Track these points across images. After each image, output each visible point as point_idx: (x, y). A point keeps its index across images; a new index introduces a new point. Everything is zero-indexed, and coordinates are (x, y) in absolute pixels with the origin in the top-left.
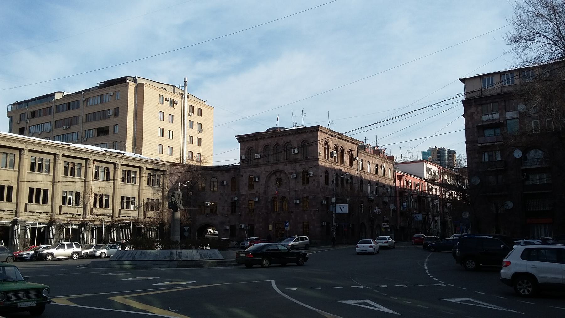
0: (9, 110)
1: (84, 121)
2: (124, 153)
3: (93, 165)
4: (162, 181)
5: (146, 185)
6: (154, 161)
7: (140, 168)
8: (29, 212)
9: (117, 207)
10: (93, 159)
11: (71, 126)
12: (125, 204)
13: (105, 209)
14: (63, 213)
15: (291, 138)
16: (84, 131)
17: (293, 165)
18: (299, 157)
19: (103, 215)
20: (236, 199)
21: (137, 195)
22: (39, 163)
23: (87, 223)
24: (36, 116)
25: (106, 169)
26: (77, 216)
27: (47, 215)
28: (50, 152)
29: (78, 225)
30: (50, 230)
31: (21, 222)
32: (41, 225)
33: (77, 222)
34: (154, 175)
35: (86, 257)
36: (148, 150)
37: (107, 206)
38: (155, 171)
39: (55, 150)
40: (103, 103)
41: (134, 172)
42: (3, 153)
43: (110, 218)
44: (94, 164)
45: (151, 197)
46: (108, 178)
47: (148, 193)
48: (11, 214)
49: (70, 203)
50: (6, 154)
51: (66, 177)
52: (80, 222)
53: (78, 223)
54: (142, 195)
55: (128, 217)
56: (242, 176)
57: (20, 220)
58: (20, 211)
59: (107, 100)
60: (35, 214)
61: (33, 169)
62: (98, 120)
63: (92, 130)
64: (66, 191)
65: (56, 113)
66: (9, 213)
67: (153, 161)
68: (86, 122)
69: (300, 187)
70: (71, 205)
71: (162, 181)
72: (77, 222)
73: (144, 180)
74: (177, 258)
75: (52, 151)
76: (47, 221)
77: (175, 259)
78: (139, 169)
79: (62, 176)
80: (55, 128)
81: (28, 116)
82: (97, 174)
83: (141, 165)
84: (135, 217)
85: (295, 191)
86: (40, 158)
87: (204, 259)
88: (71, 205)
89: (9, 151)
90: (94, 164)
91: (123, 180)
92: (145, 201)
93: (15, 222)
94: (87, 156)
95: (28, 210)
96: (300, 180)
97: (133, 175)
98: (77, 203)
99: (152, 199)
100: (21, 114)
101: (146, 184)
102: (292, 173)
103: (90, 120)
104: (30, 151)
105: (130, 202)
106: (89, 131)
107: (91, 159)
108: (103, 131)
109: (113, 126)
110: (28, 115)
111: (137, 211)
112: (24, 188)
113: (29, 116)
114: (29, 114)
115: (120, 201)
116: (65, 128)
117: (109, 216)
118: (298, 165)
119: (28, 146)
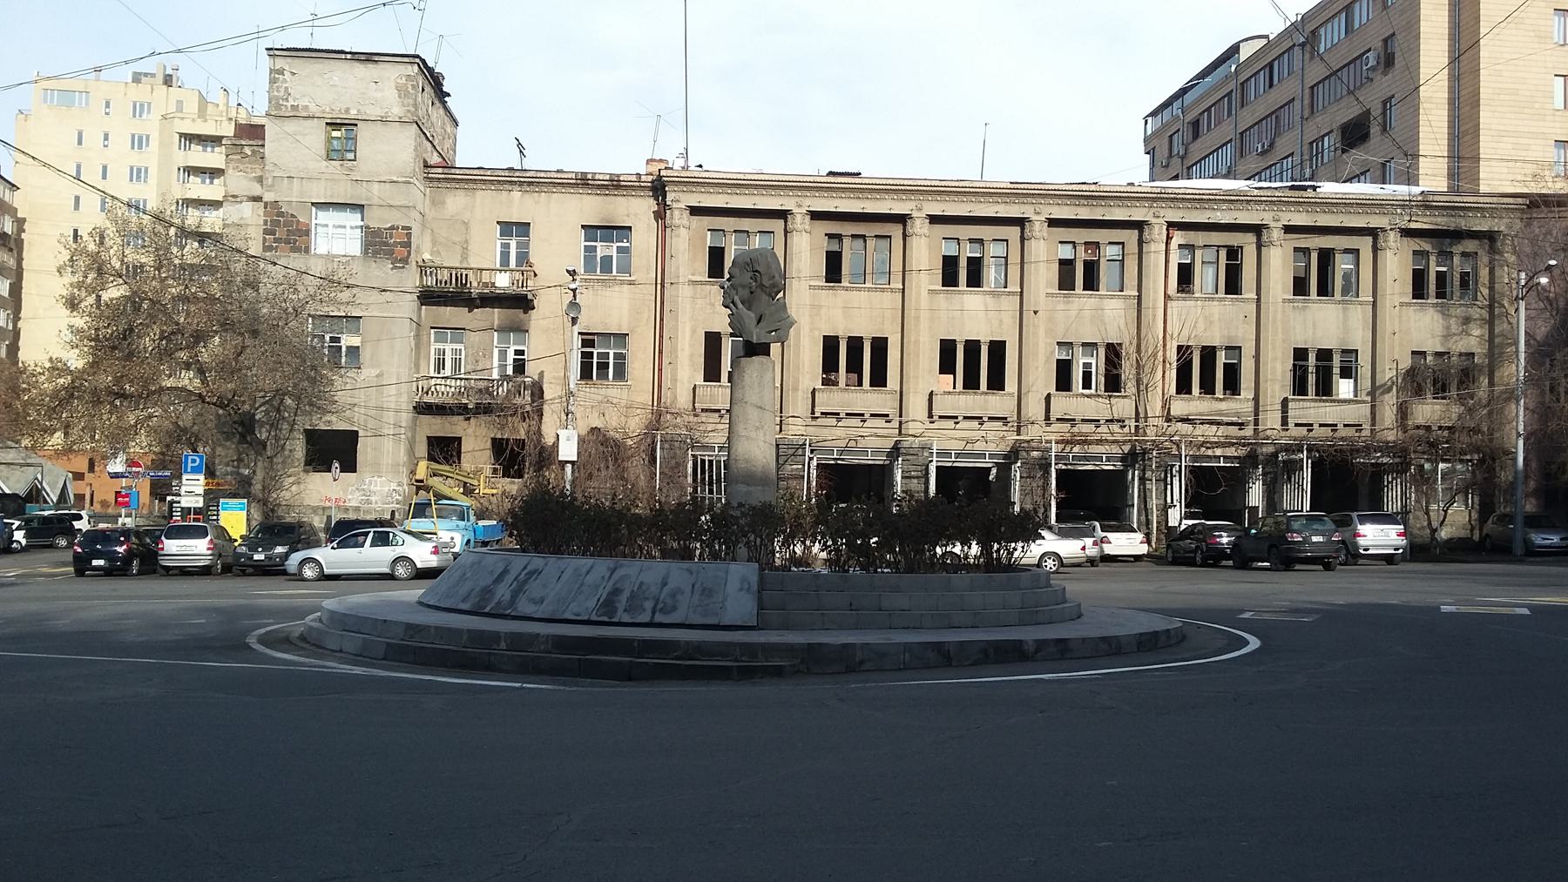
0: (1149, 132)
1: (1306, 114)
2: (1314, 188)
3: (1167, 244)
4: (1484, 273)
5: (1408, 298)
6: (1436, 198)
7: (1373, 233)
8: (940, 417)
9: (1273, 391)
10: (1161, 221)
11: (1276, 139)
12: (1312, 379)
13: (1221, 400)
14: (1058, 419)
16: (1306, 147)
19: (1211, 423)
21: (1363, 342)
22: (968, 257)
23: (1145, 452)
24: (1201, 133)
25: (1223, 253)
26: (1115, 428)
27: (1005, 428)
28: (998, 215)
29: (1123, 459)
30: (1386, 484)
31: (911, 451)
32: (987, 460)
33: (1115, 449)
34: (1445, 256)
35: (1054, 569)
36: (1506, 170)
37: (1232, 385)
38: (1448, 240)
39: (1016, 206)
40: (1353, 31)
41: (1347, 251)
42: (854, 236)
43: (1248, 431)
44: (1169, 238)
45: (1432, 345)
46: (1233, 285)
48: (888, 425)
49: (1087, 384)
50: (863, 237)
51: (1065, 296)
52: (1127, 448)
53: (1121, 452)
54: (1383, 339)
55: (1321, 425)
57: (905, 444)
58: (908, 415)
59: (1364, 20)
60: (964, 424)
61: (949, 279)
62: (1342, 98)
63: (1326, 139)
64: (1072, 343)
65: (1243, 106)
66: (880, 422)
67: (1431, 198)
68: (1313, 113)
70: (1093, 391)
71: (1484, 273)
72: (1115, 449)
73: (1389, 281)
74: (499, 603)
75: (1007, 213)
76: (1004, 448)
77: (486, 610)
78: (1370, 239)
79: (1050, 291)
80: (1242, 156)
81: (1185, 138)
82: (1186, 276)
83: (1375, 222)
84: (1358, 427)
86: (971, 241)
87: (615, 620)
88: (1093, 391)
89: (869, 229)
90: (1169, 238)
91: (1300, 287)
92: (1406, 363)
93: (895, 451)
94: (1137, 215)
95: (937, 412)
97: (1343, 265)
98: (1113, 384)
99: (1438, 354)
100: (1171, 136)
101: (1402, 294)
103: (1320, 108)
104: (934, 220)
105: (1336, 370)
106: (1320, 143)
107: (1154, 220)
108: (1354, 134)
109: (1380, 106)
110: (1185, 134)
111: (1364, 402)
112: (917, 342)
113: (1189, 135)
114: (1185, 129)
115: (1291, 367)
116: (1259, 151)
117: (1241, 425)
119: (924, 204)
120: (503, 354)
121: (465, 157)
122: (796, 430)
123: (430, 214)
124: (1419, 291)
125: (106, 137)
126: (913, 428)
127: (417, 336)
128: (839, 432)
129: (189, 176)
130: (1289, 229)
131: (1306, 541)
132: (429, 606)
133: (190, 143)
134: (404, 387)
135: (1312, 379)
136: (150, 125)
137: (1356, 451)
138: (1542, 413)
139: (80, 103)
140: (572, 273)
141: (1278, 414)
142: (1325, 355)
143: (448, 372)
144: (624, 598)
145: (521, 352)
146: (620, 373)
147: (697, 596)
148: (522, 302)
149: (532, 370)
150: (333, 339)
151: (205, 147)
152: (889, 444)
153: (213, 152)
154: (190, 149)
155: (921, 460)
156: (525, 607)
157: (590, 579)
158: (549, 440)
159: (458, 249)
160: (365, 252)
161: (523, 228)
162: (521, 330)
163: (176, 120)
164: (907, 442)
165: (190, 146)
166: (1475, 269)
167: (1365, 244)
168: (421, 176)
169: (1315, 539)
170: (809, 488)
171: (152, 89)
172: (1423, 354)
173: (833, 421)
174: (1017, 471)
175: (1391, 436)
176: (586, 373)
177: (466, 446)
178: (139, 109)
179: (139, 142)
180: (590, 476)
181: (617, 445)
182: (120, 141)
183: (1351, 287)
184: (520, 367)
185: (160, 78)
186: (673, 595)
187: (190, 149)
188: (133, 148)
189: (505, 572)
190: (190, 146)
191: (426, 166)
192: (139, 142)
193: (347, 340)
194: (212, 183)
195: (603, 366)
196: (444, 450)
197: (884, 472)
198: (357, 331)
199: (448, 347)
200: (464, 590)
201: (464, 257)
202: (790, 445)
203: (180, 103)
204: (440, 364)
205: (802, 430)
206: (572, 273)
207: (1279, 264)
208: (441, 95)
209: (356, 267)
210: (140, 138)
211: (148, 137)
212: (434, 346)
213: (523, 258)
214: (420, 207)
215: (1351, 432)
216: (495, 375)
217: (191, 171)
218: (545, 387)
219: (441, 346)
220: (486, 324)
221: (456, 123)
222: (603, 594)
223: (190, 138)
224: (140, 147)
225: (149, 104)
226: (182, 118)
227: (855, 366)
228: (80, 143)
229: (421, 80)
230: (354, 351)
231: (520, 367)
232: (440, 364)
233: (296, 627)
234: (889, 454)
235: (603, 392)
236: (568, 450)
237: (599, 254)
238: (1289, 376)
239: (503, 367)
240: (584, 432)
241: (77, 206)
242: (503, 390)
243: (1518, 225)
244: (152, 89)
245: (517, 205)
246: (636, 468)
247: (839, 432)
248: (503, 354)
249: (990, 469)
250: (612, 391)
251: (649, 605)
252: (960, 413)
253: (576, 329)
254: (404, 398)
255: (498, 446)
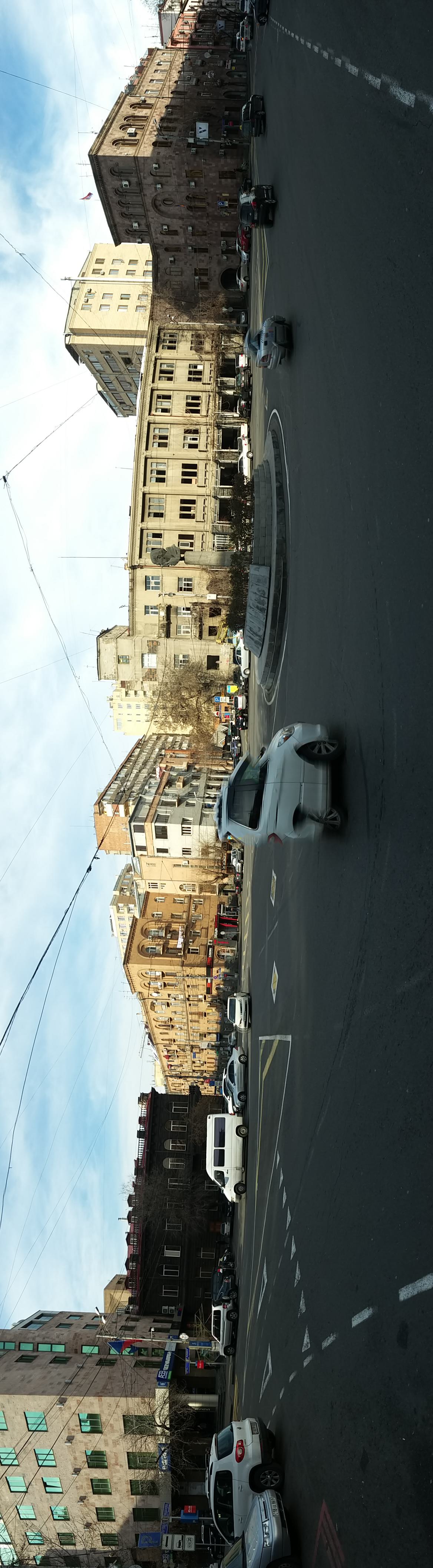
5: (175, 351)
12: (197, 376)
15: (109, 188)
17: (145, 187)
18: (134, 180)
20: (190, 248)
41: (161, 366)
47: (184, 348)
56: (163, 241)
66: (206, 502)
69: (174, 180)
85: (179, 185)
91: (170, 379)
92: (194, 352)
93: (215, 497)
95: (203, 485)
96: (164, 180)
97: (165, 367)
102: (156, 188)
105: (195, 370)
118: (145, 181)
120: (184, 614)
121: (126, 623)
122: (208, 526)
123: (143, 635)
124: (174, 348)
126: (208, 492)
127: (179, 639)
128: (209, 514)
130: (153, 382)
131: (244, 382)
132: (260, 655)
134: (194, 643)
135: (197, 376)
137: (218, 366)
138: (209, 318)
140: (160, 595)
141: (207, 385)
142: (190, 373)
143: (189, 630)
144: (259, 605)
145: (184, 609)
146: (190, 580)
147: (260, 584)
148: (169, 608)
149: (189, 606)
150: (181, 662)
152: (213, 499)
155: (218, 490)
156: (261, 633)
157: (253, 614)
158: (210, 602)
159: (153, 627)
160: (155, 653)
161: (146, 607)
162: (177, 609)
164: (212, 494)
166: (168, 333)
167: (159, 362)
168: (132, 637)
169: (243, 379)
170: (226, 524)
172: (191, 347)
173: (206, 516)
174: (222, 461)
175: (214, 356)
176: (190, 590)
177: (212, 625)
180: (221, 590)
181: (211, 582)
183: (171, 365)
184: (188, 609)
186: (259, 591)
189: (250, 637)
191: (129, 635)
193: (181, 658)
195: (188, 585)
196: (213, 631)
197: (221, 500)
198: (178, 656)
199: (182, 630)
200: (255, 648)
201: (156, 625)
202: (213, 529)
204: (188, 632)
205: (208, 525)
206: (160, 595)
207: (163, 385)
208: (108, 631)
209: (160, 656)
212: (182, 634)
213: (155, 608)
214: (141, 638)
215: (213, 366)
216: (190, 616)
218: (194, 601)
219: (182, 632)
220: (175, 619)
221: (116, 626)
222: (258, 611)
227: (189, 509)
229: (104, 637)
230: (184, 657)
231: (188, 609)
232: (188, 632)
233: (265, 691)
234: (216, 499)
235: (196, 585)
236: (213, 597)
237: (154, 585)
238: (196, 382)
239: (188, 614)
240: (208, 592)
242: (195, 614)
243: (157, 323)
245: (139, 609)
246: (220, 576)
247: (209, 514)
248: (184, 614)
249: (221, 469)
250: (195, 582)
251: (262, 599)
252: (204, 478)
253: (177, 594)
254: (197, 643)
255: (212, 616)
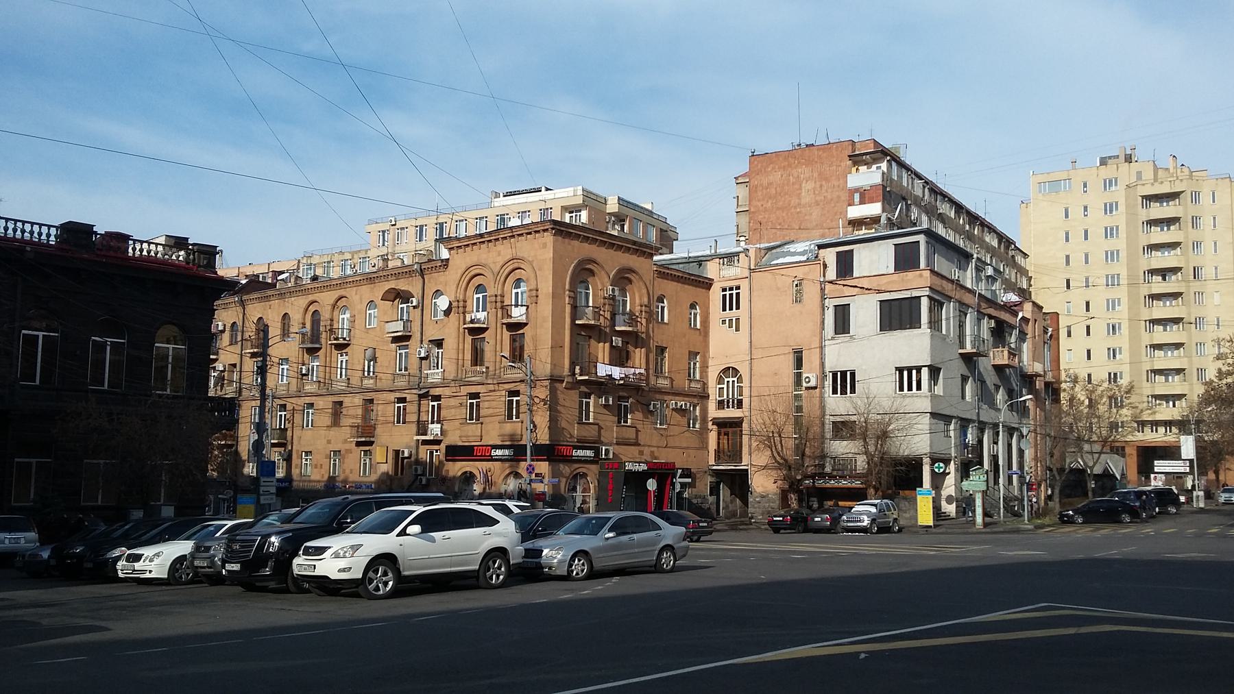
125: (1086, 208)
129: (1150, 228)
133: (1150, 202)
136: (1118, 194)
139: (1065, 188)
151: (1161, 203)
153: (1168, 205)
154: (1150, 206)
163: (1138, 187)
165: (1150, 204)
171: (1118, 168)
178: (1109, 183)
179: (1110, 208)
182: (1096, 212)
185: (1122, 158)
187: (1150, 206)
188: (1106, 213)
190: (1150, 204)
192: (1110, 208)
194: (1169, 229)
203: (1139, 174)
210: (1111, 205)
211: (1117, 203)
217: (1153, 223)
223: (1150, 198)
224: (1111, 211)
225: (1116, 179)
226: (1143, 185)
228: (1067, 216)
241: (1068, 262)
244: (1118, 168)
